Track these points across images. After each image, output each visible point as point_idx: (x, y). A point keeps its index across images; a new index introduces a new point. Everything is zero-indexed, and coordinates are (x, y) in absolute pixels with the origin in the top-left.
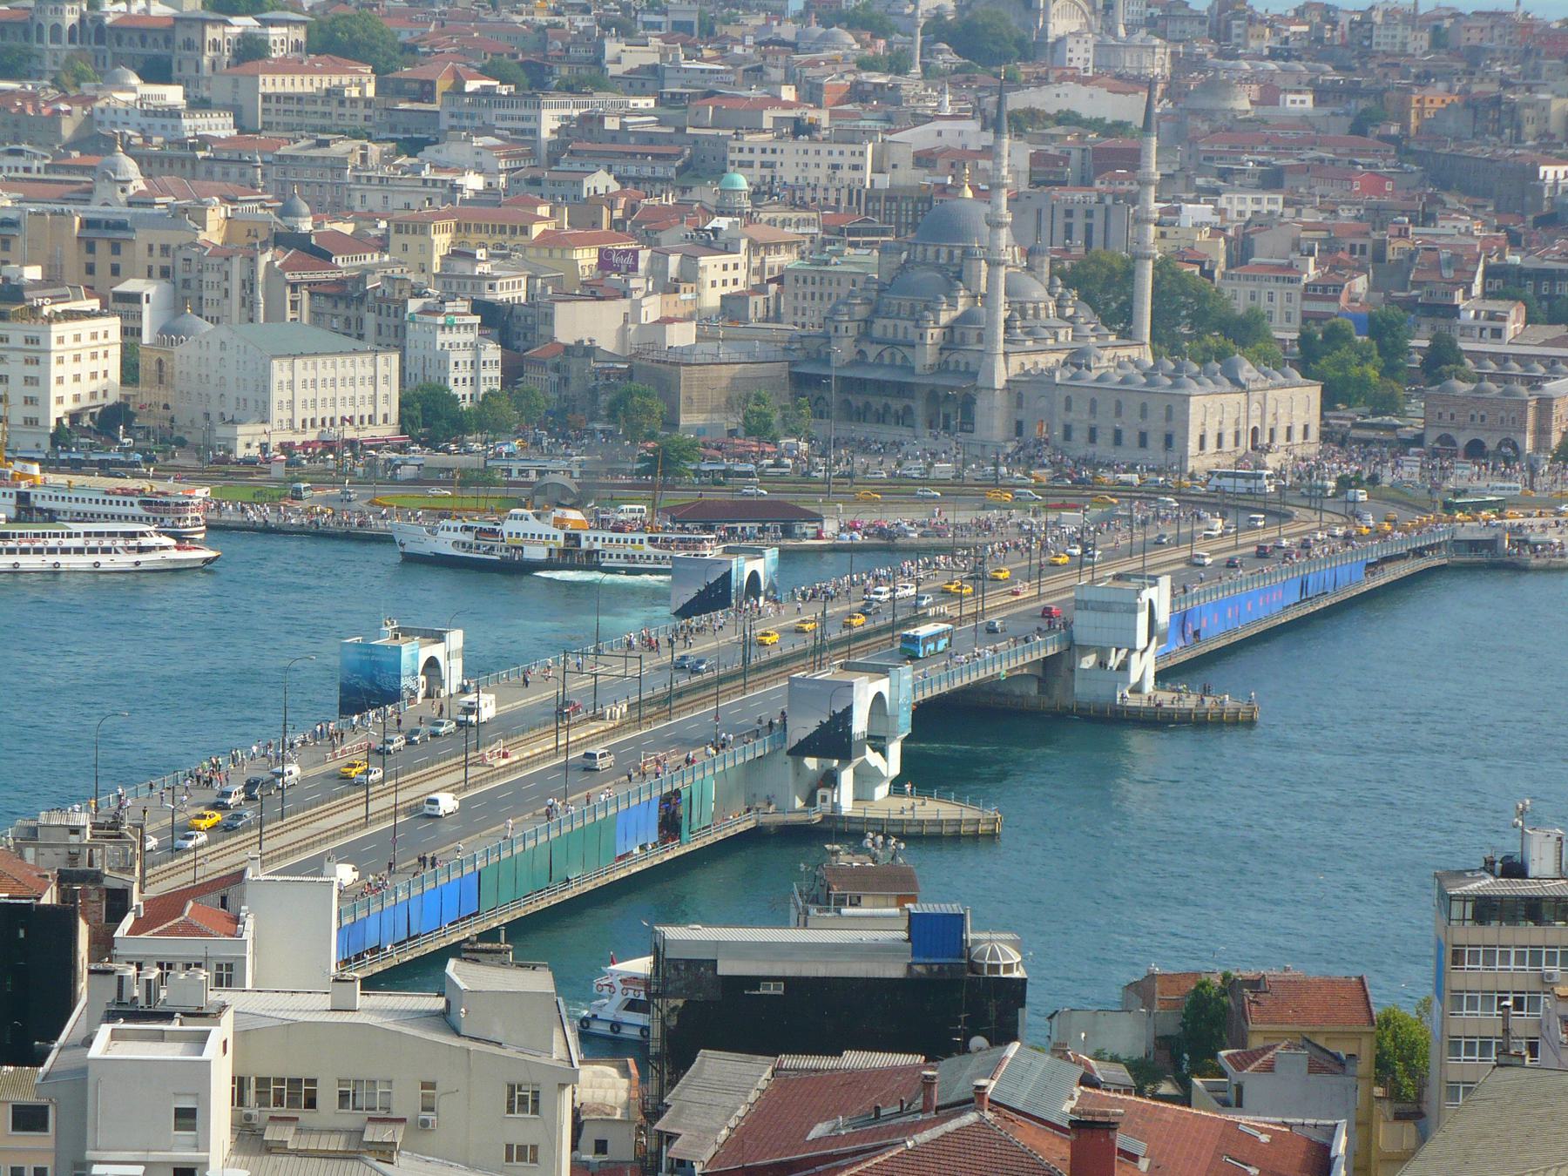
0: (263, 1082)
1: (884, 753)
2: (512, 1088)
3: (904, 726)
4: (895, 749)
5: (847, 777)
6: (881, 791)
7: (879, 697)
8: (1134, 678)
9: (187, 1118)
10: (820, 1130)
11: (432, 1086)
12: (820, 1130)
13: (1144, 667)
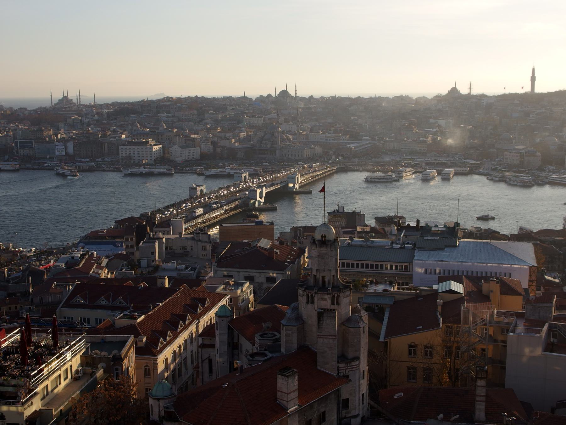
0: (170, 247)
1: (262, 199)
2: (202, 247)
3: (264, 195)
4: (263, 198)
5: (257, 202)
6: (262, 204)
7: (260, 191)
8: (296, 187)
9: (153, 253)
10: (236, 251)
11: (192, 247)
12: (236, 251)
13: (297, 186)
